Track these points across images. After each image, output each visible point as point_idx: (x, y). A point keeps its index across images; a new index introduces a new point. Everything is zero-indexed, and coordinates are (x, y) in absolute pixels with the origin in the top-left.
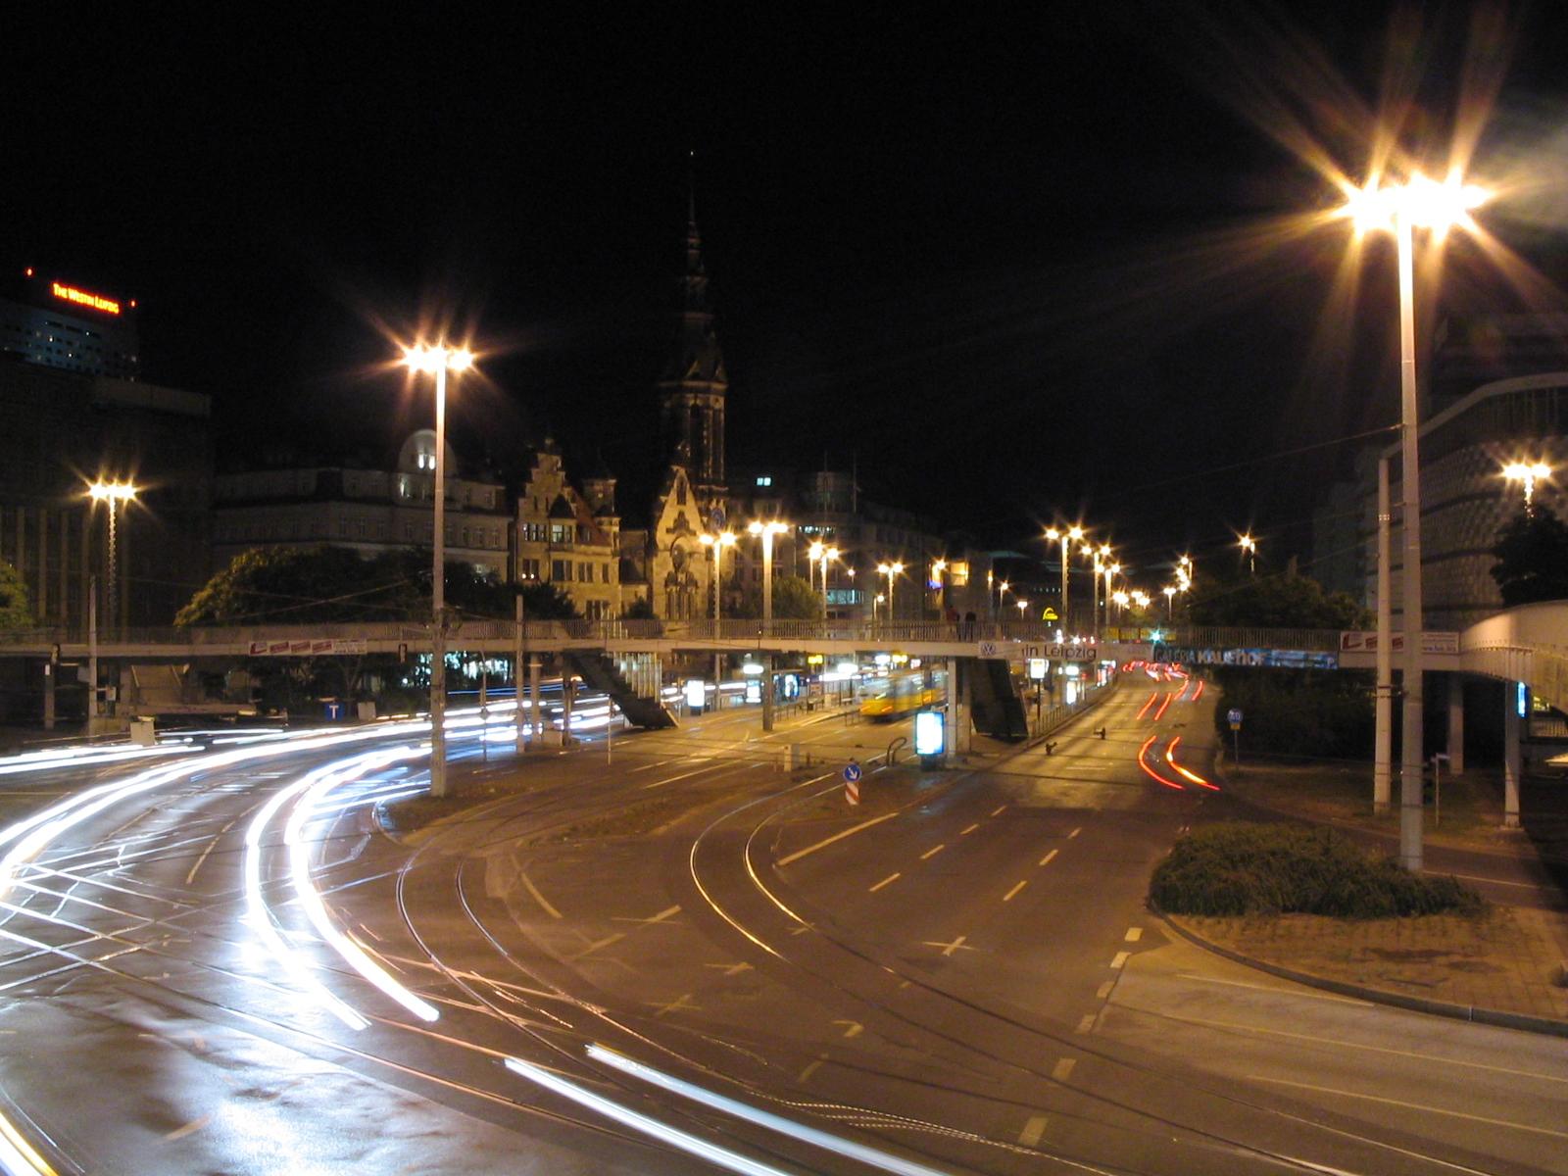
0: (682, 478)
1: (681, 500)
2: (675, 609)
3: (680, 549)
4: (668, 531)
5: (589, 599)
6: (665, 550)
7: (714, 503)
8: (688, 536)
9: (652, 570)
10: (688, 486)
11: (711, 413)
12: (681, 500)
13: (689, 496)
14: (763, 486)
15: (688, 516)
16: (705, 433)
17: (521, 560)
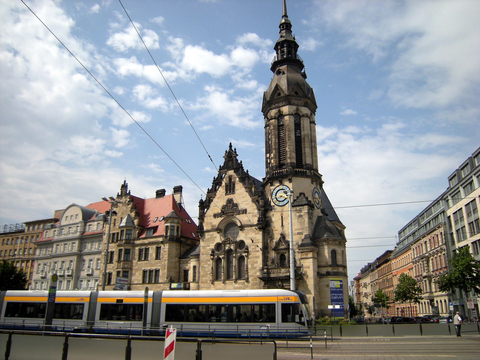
4: (215, 216)
5: (143, 269)
8: (237, 216)
10: (237, 179)
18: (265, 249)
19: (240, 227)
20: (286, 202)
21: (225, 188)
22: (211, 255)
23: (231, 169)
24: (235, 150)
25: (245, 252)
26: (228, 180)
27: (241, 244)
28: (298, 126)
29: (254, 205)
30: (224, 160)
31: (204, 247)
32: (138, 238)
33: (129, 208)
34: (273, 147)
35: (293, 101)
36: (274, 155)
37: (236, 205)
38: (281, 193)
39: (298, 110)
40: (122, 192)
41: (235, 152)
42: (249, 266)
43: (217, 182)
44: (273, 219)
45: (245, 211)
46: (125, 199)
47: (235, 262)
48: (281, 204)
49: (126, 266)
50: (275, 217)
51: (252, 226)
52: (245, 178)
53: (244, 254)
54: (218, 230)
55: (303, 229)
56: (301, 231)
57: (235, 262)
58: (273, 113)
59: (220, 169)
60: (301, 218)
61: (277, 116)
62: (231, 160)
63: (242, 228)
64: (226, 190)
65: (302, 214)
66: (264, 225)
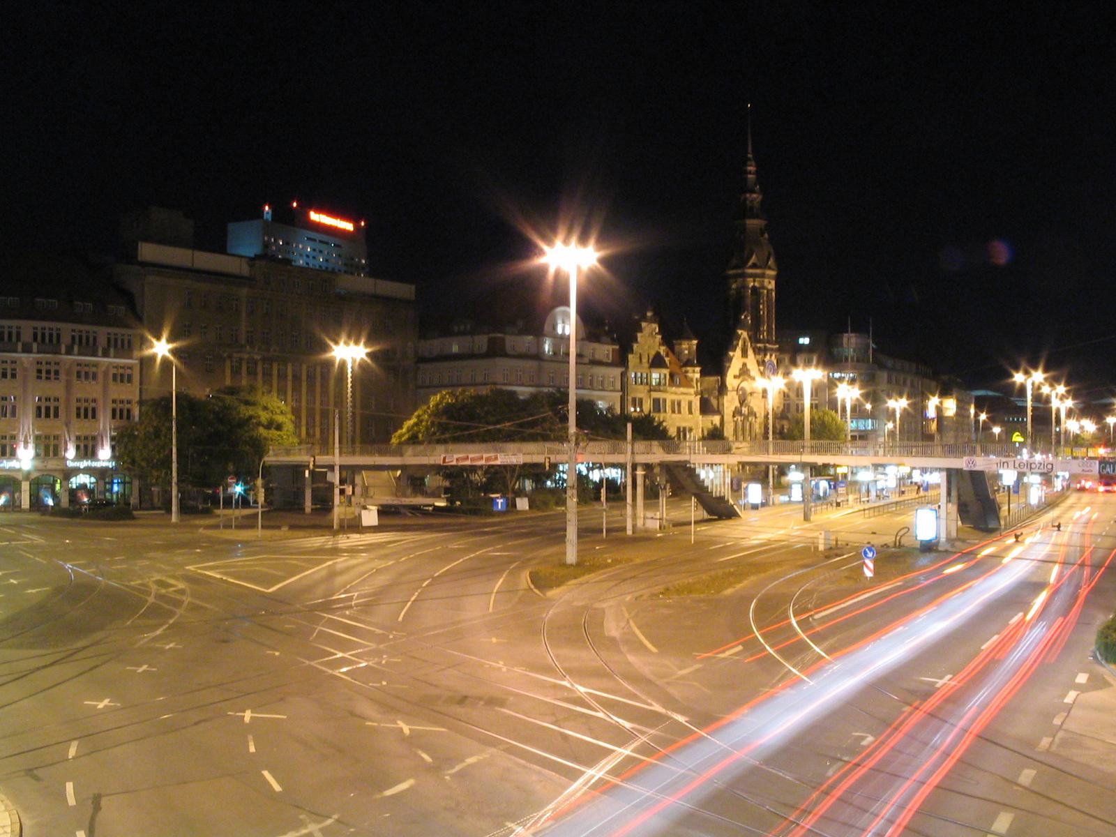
0: (744, 339)
1: (744, 354)
2: (740, 433)
3: (743, 389)
4: (735, 377)
6: (733, 390)
7: (768, 357)
8: (749, 380)
9: (723, 405)
11: (765, 291)
12: (744, 354)
13: (750, 352)
14: (803, 345)
15: (749, 366)
16: (761, 307)
17: (630, 398)
51: (758, 393)
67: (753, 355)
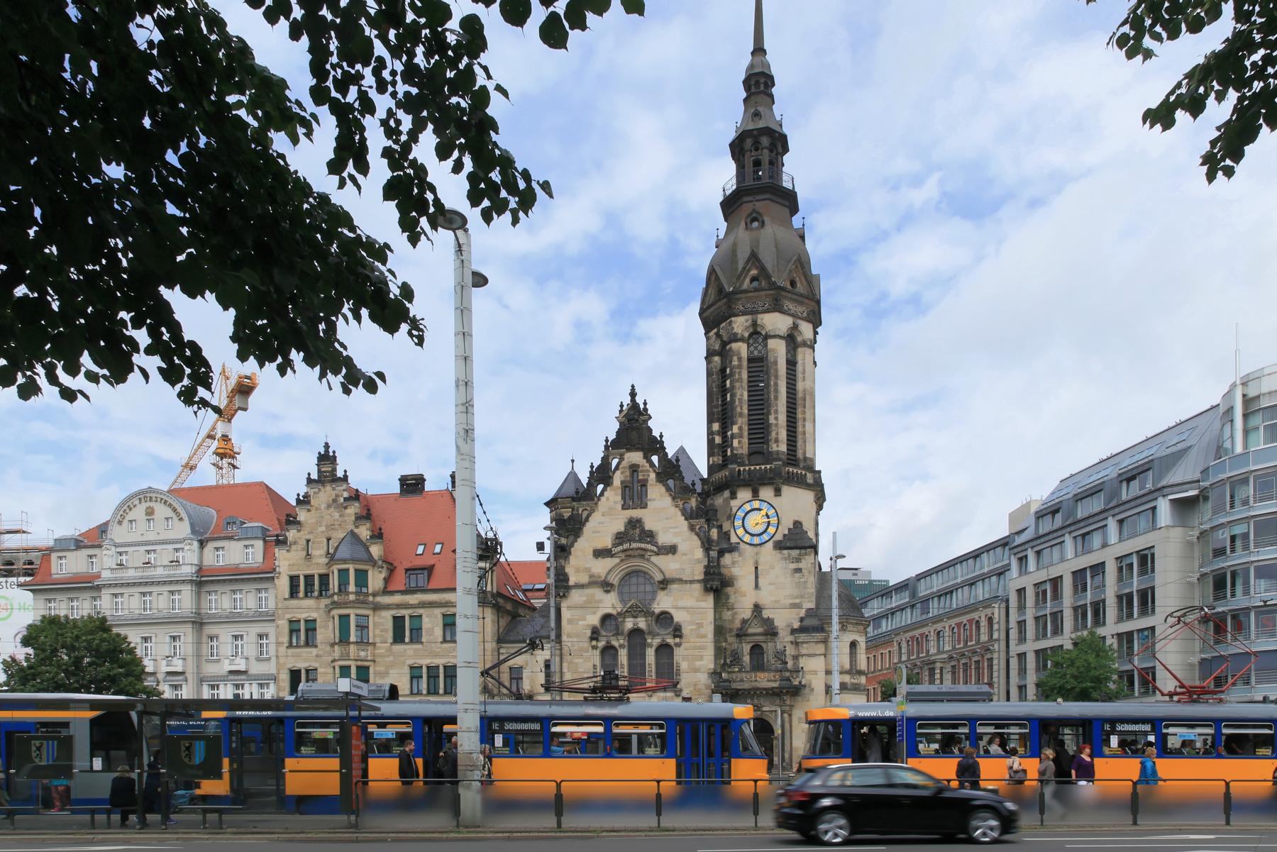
0: (634, 468)
4: (600, 553)
5: (410, 662)
7: (744, 495)
8: (654, 559)
10: (653, 476)
18: (720, 631)
19: (661, 582)
20: (765, 537)
21: (620, 491)
22: (592, 639)
23: (637, 450)
24: (645, 404)
25: (675, 636)
26: (628, 473)
27: (664, 618)
28: (791, 363)
29: (696, 538)
30: (617, 426)
31: (570, 621)
32: (385, 592)
33: (349, 515)
34: (739, 409)
35: (788, 305)
36: (740, 428)
37: (649, 536)
38: (754, 516)
39: (795, 327)
40: (319, 471)
41: (645, 409)
42: (684, 666)
43: (602, 474)
44: (735, 571)
45: (672, 550)
46: (334, 493)
47: (650, 656)
48: (756, 540)
49: (362, 654)
50: (739, 567)
52: (672, 470)
53: (670, 641)
54: (606, 586)
55: (802, 597)
56: (797, 601)
57: (650, 656)
58: (740, 324)
59: (606, 447)
60: (797, 575)
61: (746, 335)
62: (634, 428)
63: (665, 584)
64: (623, 498)
65: (800, 565)
66: (717, 584)
67: (668, 500)
